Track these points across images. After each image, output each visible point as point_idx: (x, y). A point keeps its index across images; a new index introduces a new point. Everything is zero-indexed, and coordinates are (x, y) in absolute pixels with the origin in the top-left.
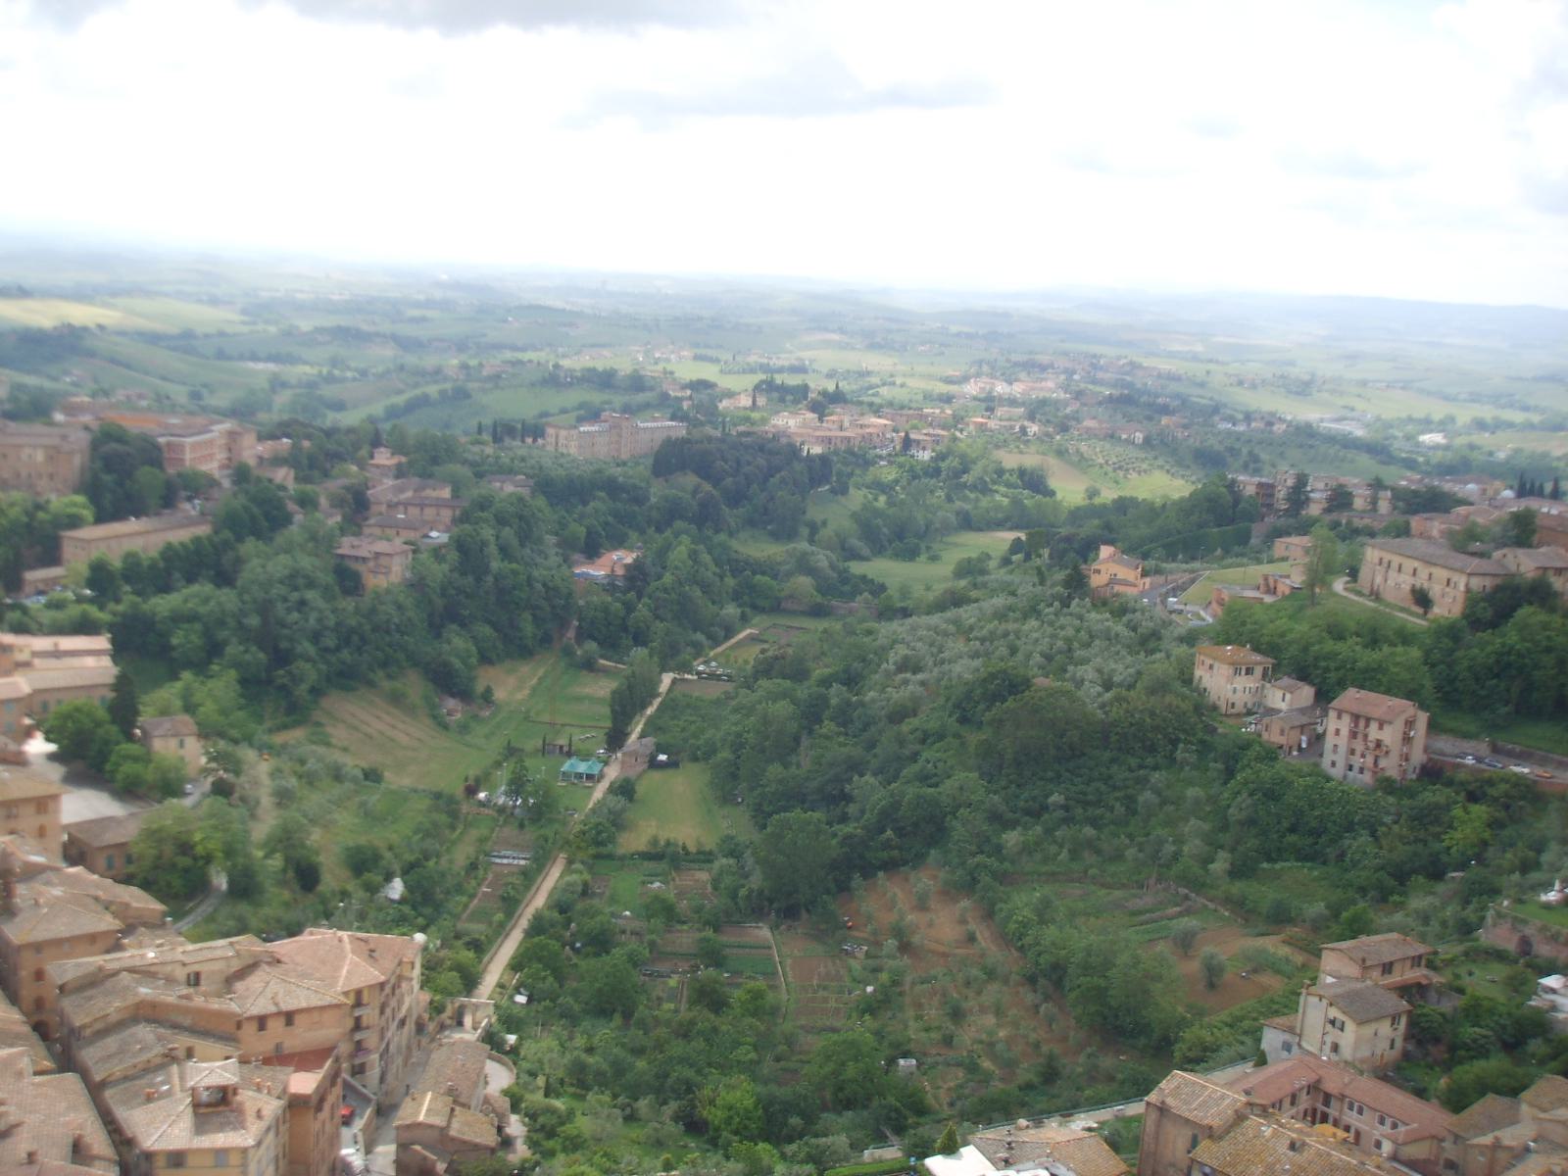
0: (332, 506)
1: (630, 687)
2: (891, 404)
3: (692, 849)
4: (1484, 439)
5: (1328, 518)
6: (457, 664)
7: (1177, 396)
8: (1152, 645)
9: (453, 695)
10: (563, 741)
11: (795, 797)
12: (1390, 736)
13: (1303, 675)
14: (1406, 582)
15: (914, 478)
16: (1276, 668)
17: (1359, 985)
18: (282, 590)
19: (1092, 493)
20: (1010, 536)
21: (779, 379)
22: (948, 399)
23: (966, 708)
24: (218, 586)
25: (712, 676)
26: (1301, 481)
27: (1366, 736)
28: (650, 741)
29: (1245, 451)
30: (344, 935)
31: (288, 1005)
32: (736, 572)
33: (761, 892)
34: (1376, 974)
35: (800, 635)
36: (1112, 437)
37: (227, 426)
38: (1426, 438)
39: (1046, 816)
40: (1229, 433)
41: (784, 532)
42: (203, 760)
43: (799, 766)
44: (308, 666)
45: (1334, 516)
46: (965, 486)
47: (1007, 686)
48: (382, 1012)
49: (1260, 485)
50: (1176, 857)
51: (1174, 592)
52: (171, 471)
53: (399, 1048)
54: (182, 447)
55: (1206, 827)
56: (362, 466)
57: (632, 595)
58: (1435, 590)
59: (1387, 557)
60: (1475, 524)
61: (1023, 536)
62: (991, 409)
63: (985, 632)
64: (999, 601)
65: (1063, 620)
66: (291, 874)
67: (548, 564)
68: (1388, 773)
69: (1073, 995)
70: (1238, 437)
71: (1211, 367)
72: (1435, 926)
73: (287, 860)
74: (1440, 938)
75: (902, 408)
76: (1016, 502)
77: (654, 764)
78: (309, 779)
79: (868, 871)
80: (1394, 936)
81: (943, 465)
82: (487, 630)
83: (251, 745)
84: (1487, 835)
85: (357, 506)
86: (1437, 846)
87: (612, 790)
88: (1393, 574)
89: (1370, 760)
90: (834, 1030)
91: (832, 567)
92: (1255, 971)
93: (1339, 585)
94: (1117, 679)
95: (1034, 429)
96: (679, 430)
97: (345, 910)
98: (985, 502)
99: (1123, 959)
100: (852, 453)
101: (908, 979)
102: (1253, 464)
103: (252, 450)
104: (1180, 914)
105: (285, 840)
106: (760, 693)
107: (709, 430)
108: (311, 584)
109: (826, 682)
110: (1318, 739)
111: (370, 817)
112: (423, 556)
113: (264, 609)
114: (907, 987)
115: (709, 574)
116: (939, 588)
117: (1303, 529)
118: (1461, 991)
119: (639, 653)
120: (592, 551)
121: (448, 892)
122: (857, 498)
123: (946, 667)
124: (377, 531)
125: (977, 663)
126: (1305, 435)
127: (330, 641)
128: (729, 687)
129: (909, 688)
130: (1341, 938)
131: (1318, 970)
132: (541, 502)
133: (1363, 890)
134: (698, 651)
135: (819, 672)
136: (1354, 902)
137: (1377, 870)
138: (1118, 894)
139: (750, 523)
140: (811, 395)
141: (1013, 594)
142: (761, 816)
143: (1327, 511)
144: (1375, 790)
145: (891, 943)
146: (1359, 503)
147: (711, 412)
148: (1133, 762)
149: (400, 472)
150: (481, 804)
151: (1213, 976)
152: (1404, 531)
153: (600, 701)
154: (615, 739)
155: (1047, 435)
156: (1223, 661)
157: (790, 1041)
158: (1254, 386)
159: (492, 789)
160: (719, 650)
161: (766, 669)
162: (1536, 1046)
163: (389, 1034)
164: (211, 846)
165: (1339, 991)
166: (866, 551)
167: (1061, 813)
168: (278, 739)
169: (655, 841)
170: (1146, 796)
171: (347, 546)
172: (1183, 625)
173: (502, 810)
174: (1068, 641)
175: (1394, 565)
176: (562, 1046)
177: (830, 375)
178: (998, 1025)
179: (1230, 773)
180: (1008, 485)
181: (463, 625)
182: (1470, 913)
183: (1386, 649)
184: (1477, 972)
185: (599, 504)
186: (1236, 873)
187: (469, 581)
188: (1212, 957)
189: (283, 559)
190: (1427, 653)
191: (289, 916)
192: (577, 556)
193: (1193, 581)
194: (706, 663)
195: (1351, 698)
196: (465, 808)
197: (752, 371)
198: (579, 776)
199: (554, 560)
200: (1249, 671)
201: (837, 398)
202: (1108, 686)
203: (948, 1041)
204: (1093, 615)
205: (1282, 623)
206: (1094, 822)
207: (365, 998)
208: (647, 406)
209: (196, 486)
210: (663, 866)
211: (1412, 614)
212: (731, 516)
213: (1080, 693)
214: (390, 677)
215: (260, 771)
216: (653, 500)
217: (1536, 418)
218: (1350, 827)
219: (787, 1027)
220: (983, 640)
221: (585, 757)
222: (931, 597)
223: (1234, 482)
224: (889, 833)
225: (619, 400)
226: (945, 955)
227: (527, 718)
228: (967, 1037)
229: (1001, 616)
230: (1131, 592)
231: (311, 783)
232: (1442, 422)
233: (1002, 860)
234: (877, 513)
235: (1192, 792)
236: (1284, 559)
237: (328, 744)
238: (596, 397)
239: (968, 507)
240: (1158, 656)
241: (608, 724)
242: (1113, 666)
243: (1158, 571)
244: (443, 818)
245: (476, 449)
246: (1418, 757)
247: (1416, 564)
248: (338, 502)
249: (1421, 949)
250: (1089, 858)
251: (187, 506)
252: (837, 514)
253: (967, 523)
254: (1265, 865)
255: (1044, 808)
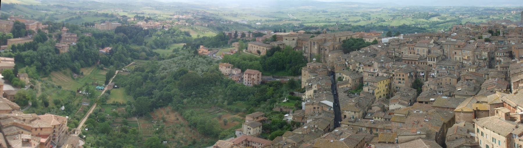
0: (55, 37)
1: (110, 73)
2: (160, 20)
3: (122, 103)
4: (267, 23)
5: (241, 39)
6: (77, 67)
7: (213, 17)
8: (211, 63)
9: (76, 73)
10: (96, 83)
11: (142, 94)
12: (255, 77)
13: (239, 67)
14: (256, 49)
15: (165, 33)
16: (234, 66)
17: (253, 121)
18: (45, 52)
19: (198, 36)
20: (183, 44)
21: (139, 15)
22: (171, 19)
23: (175, 77)
24: (34, 51)
25: (126, 71)
26: (236, 32)
27: (251, 77)
28: (113, 83)
29: (226, 27)
30: (53, 115)
31: (41, 127)
32: (131, 52)
33: (135, 111)
34: (256, 119)
35: (143, 63)
36: (202, 25)
37: (37, 22)
38: (258, 24)
39: (192, 96)
40: (223, 24)
41: (140, 44)
42: (29, 82)
43: (143, 88)
44: (49, 66)
45: (242, 38)
46: (174, 35)
47: (183, 72)
48: (59, 130)
49: (229, 33)
50: (217, 102)
51: (214, 54)
52: (27, 30)
53: (62, 137)
54: (29, 25)
55: (223, 96)
56: (61, 30)
57: (110, 56)
58: (261, 51)
59: (252, 45)
60: (267, 38)
61: (186, 44)
62: (179, 21)
63: (179, 62)
64: (182, 56)
65: (194, 60)
66: (43, 104)
67: (94, 49)
68: (255, 84)
69: (198, 129)
70: (225, 25)
71: (219, 12)
72: (266, 109)
73: (43, 101)
74: (267, 111)
75: (162, 20)
76: (184, 38)
77: (114, 87)
78: (48, 87)
79: (157, 108)
80: (258, 112)
81: (170, 31)
82: (82, 61)
83: (38, 80)
84: (273, 92)
85: (59, 37)
86: (265, 95)
87: (106, 92)
88: (253, 48)
89: (252, 82)
90: (150, 136)
91: (149, 50)
92: (233, 121)
93: (244, 51)
94: (204, 70)
95: (187, 24)
96: (120, 25)
97: (53, 111)
98: (178, 38)
99: (208, 121)
100: (152, 29)
101: (165, 127)
102: (227, 29)
103: (41, 26)
104: (218, 112)
105: (43, 97)
106: (135, 74)
107: (126, 25)
108: (50, 51)
109: (148, 72)
110: (242, 79)
111: (58, 94)
112: (71, 47)
113: (42, 55)
114: (165, 129)
115: (125, 52)
116: (170, 54)
117: (237, 41)
118: (271, 120)
119: (112, 66)
120: (103, 47)
121: (73, 109)
122: (154, 37)
123: (171, 69)
124: (63, 42)
125: (177, 68)
126: (236, 24)
127: (53, 62)
128: (129, 73)
129: (165, 73)
130: (249, 114)
131: (245, 120)
132: (93, 38)
133: (252, 105)
134: (123, 66)
135: (147, 70)
136: (251, 107)
137: (254, 101)
138: (206, 110)
139: (134, 42)
140: (145, 18)
141: (184, 55)
142: (135, 97)
143: (241, 37)
144: (253, 87)
145: (162, 121)
146: (247, 36)
147: (126, 21)
148: (208, 85)
149: (68, 32)
150: (80, 94)
151: (225, 123)
152: (255, 40)
153: (104, 75)
154: (107, 83)
155: (190, 25)
156: (224, 66)
157: (141, 138)
158: (227, 15)
159: (82, 91)
160: (127, 66)
161: (136, 70)
162: (285, 127)
163: (60, 134)
164: (29, 97)
165: (249, 123)
166: (156, 48)
167: (195, 96)
168: (43, 79)
169: (114, 102)
170: (211, 91)
171: (57, 45)
172: (216, 60)
173: (84, 95)
174: (195, 63)
175: (254, 47)
176: (94, 138)
177: (149, 15)
178: (184, 135)
179: (226, 86)
180: (183, 35)
181: (78, 60)
182: (272, 106)
183: (253, 62)
184: (273, 116)
185: (105, 38)
186: (229, 104)
187: (79, 52)
188: (225, 119)
189: (45, 46)
190: (261, 62)
191: (43, 111)
192: (100, 48)
193: (218, 51)
194: (124, 69)
195: (248, 71)
196: (77, 94)
197: (134, 14)
198: (99, 89)
199: (96, 49)
200: (229, 67)
201: (150, 19)
202: (203, 71)
203: (173, 138)
204: (199, 59)
205: (234, 58)
206: (201, 97)
207: (56, 127)
208: (114, 20)
209: (31, 32)
210: (116, 106)
211: (257, 55)
212: (130, 41)
213: (198, 73)
214: (64, 69)
215: (39, 85)
216: (115, 38)
217: (277, 19)
218: (249, 94)
219: (140, 136)
220: (178, 64)
221: (101, 86)
222: (168, 56)
223: (224, 33)
224: (161, 100)
225: (109, 19)
226: (172, 122)
227: (89, 78)
228: (177, 137)
229: (182, 59)
230: (206, 54)
231: (48, 88)
232: (260, 21)
233: (183, 105)
234: (158, 40)
235: (220, 90)
236: (234, 47)
237: (52, 81)
238: (104, 19)
239: (175, 39)
240: (212, 65)
241: (105, 80)
242: (203, 68)
243: (211, 50)
244: (73, 96)
245: (82, 28)
246: (260, 80)
247: (257, 46)
248: (56, 37)
249: (263, 114)
250: (200, 103)
251: (29, 36)
252: (150, 41)
253: (175, 42)
254: (234, 102)
255: (191, 95)
